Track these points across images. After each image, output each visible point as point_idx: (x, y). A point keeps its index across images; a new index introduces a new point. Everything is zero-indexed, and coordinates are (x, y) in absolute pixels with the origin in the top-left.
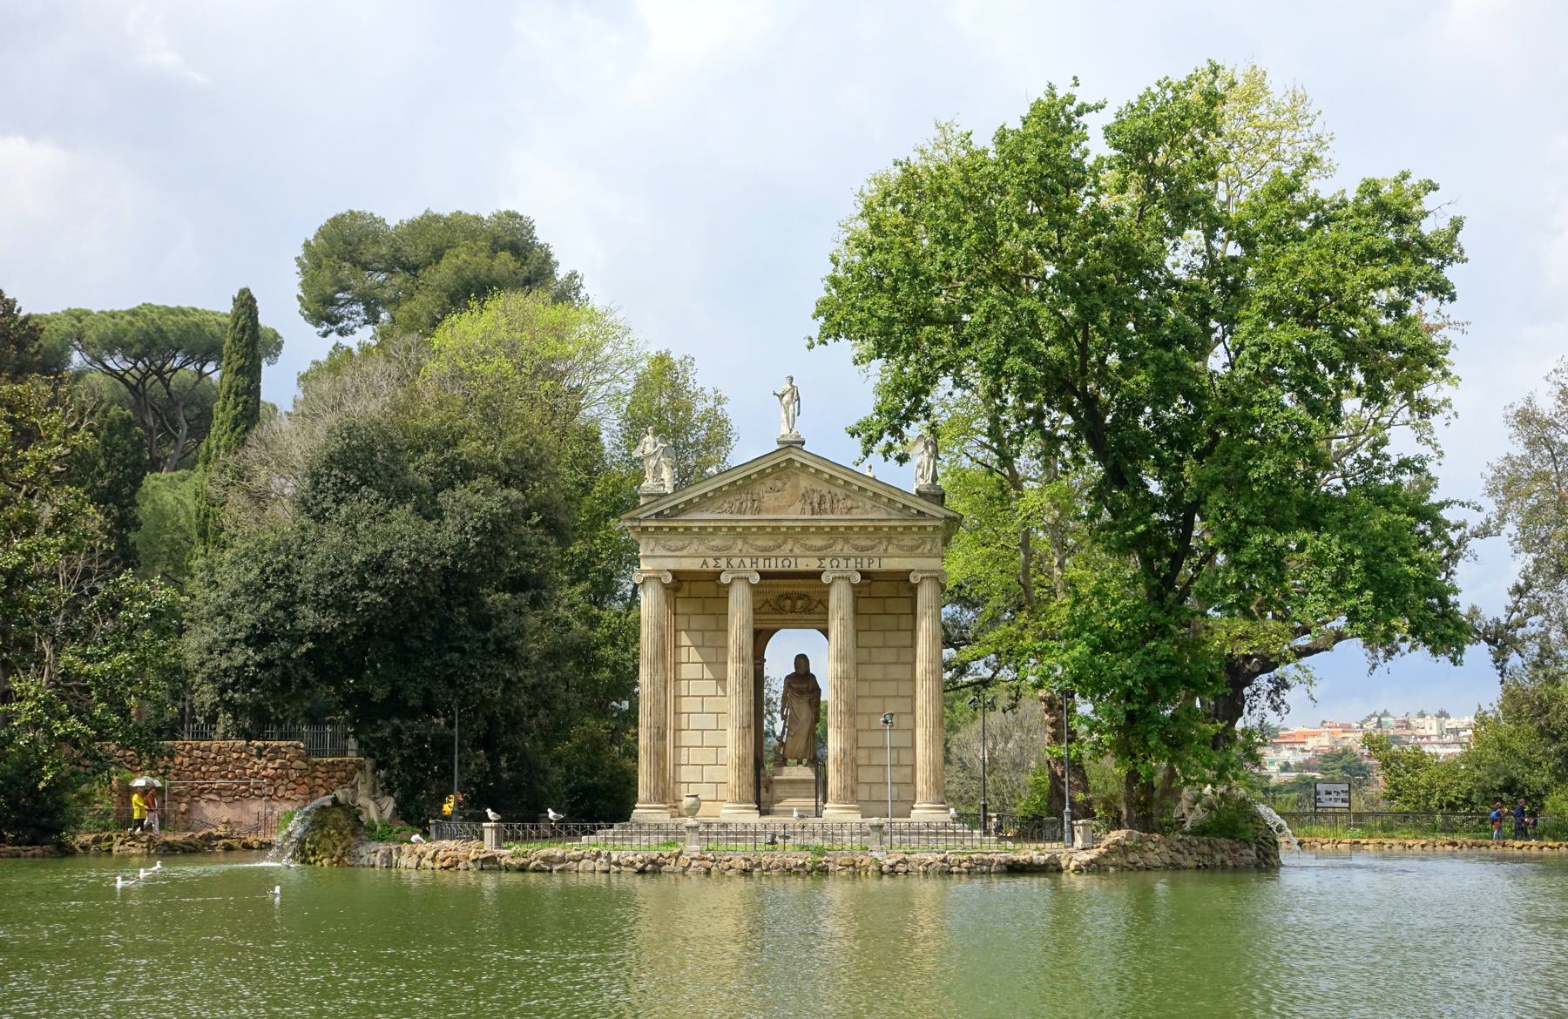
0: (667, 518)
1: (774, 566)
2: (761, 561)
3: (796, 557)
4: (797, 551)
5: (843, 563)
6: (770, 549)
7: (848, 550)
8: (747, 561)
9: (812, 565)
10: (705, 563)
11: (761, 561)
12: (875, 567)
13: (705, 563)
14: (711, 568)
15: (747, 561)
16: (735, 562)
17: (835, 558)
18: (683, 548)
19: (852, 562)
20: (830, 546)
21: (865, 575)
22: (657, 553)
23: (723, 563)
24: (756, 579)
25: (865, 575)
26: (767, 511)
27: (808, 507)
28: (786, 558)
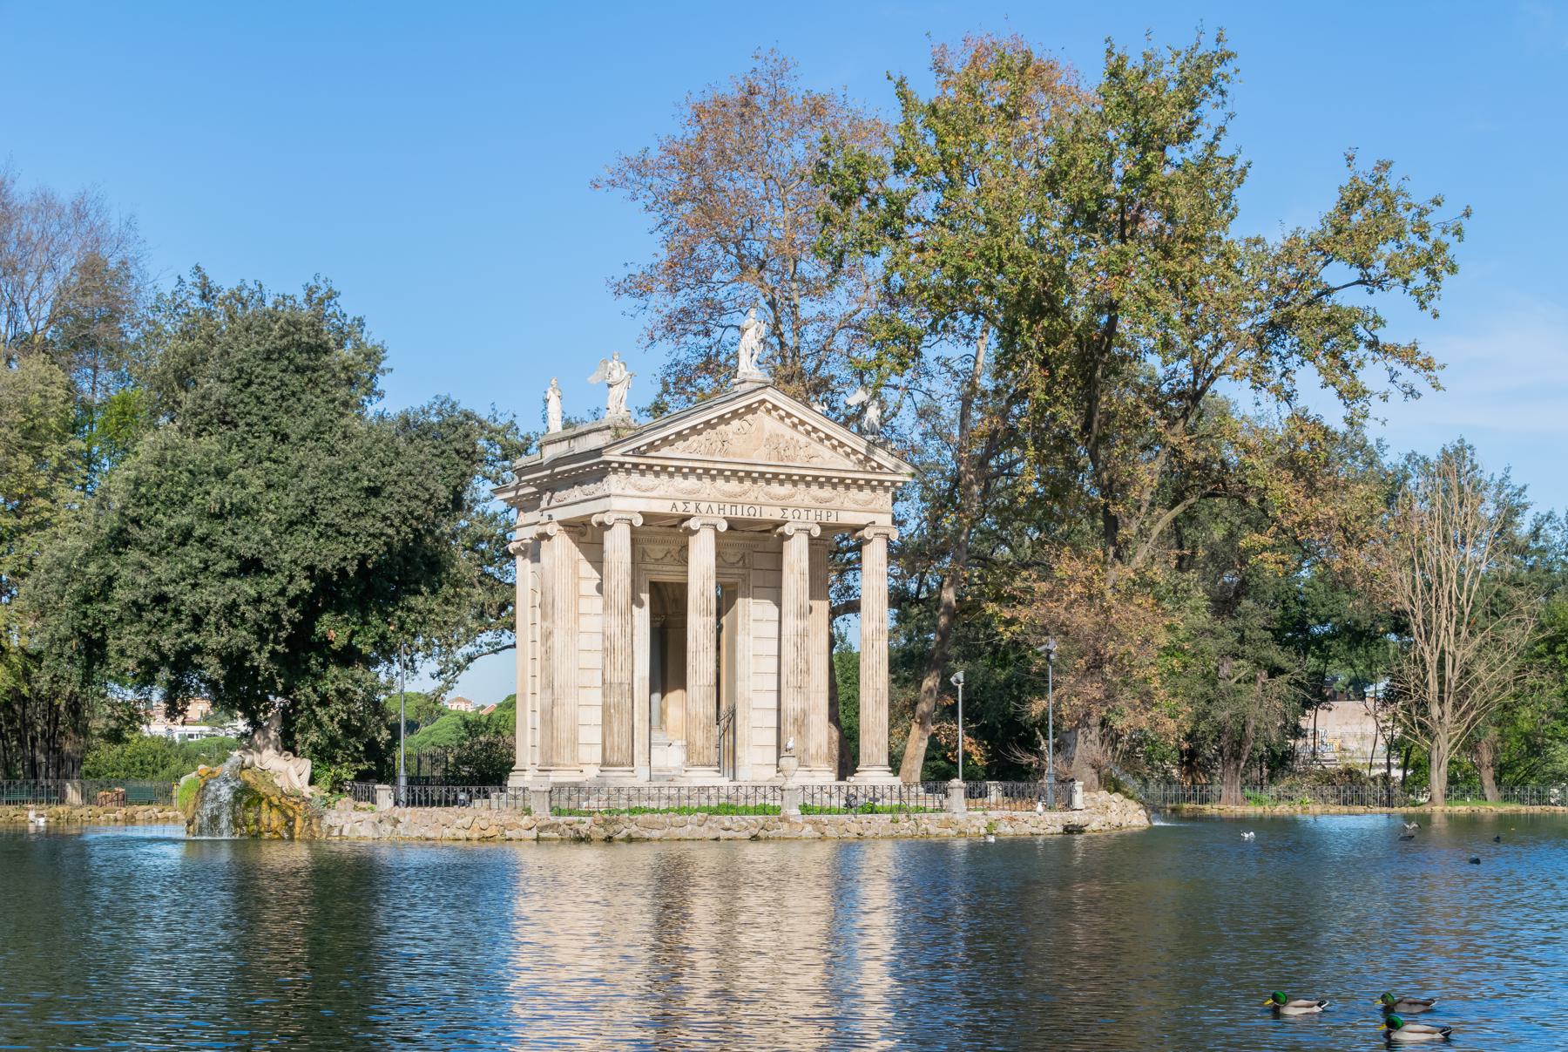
0: (643, 455)
1: (741, 513)
2: (728, 507)
3: (761, 505)
4: (762, 499)
5: (804, 514)
6: (735, 496)
7: (808, 502)
8: (715, 506)
9: (777, 515)
10: (674, 506)
11: (728, 507)
12: (832, 520)
13: (674, 506)
14: (680, 512)
15: (715, 506)
16: (703, 507)
17: (797, 508)
18: (652, 489)
19: (812, 514)
20: (792, 496)
21: (824, 527)
22: (628, 492)
23: (691, 509)
24: (723, 527)
25: (824, 527)
26: (734, 455)
27: (774, 453)
28: (752, 505)
